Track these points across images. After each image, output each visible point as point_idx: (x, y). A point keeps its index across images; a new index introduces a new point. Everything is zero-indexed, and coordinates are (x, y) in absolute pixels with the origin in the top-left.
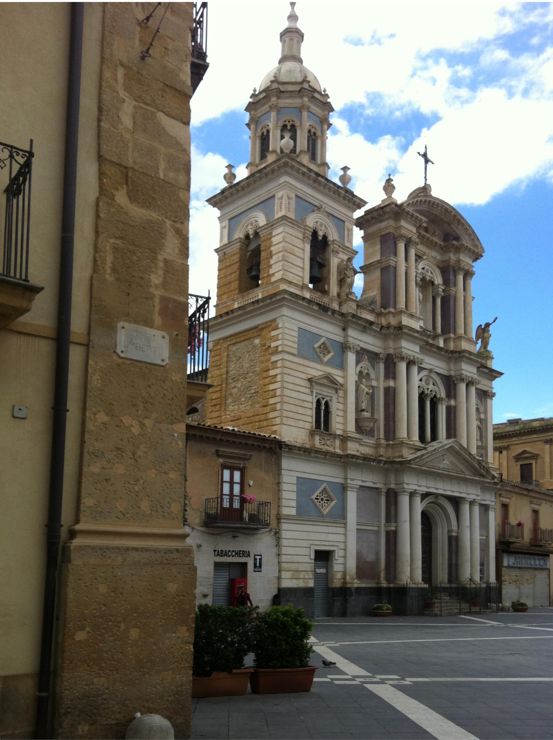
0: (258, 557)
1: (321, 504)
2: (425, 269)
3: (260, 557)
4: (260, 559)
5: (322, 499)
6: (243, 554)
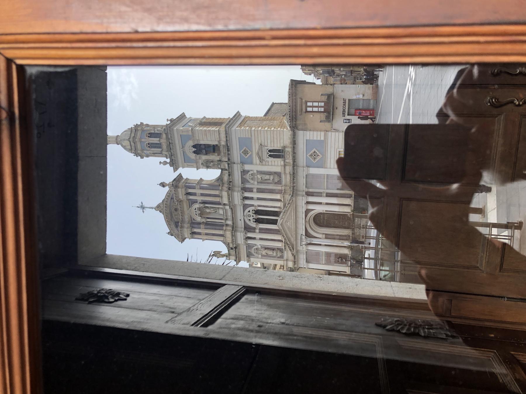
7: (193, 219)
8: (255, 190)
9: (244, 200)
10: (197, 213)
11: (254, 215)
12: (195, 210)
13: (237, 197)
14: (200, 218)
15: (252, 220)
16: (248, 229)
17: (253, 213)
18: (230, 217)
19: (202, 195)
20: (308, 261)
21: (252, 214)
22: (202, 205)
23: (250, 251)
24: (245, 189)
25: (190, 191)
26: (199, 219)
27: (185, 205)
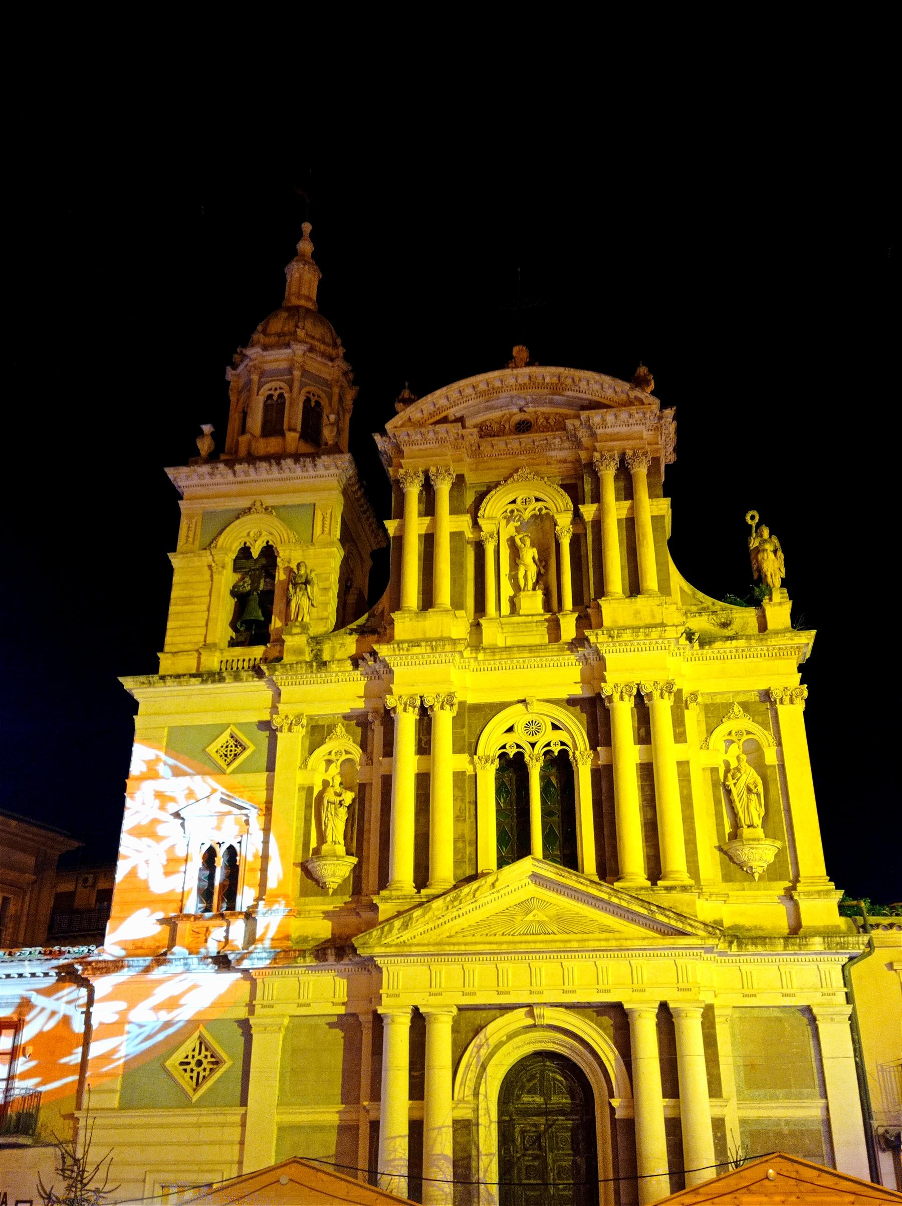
1: (195, 1075)
2: (519, 501)
15: (510, 739)
17: (548, 744)
23: (338, 729)
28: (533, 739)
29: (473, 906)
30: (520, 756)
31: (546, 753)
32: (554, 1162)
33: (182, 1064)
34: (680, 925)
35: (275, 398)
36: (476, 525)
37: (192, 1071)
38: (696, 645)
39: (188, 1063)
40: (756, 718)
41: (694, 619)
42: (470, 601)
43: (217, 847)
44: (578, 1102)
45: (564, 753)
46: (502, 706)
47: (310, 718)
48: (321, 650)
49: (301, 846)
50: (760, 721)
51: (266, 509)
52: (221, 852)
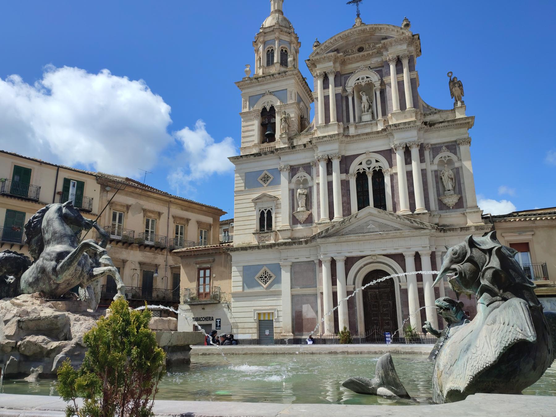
0: (218, 321)
1: (265, 280)
2: (360, 79)
3: (220, 320)
4: (220, 322)
5: (266, 277)
6: (209, 319)
7: (349, 76)
8: (424, 166)
9: (404, 149)
10: (360, 80)
11: (371, 170)
12: (365, 78)
13: (411, 136)
14: (353, 86)
15: (361, 167)
16: (346, 162)
17: (375, 168)
18: (360, 131)
19: (400, 84)
20: (293, 265)
21: (372, 166)
22: (377, 85)
23: (301, 169)
24: (422, 148)
25: (405, 63)
26: (351, 83)
27: (375, 61)
28: (369, 166)
29: (350, 224)
30: (364, 172)
31: (374, 171)
32: (382, 303)
33: (260, 277)
34: (422, 226)
35: (270, 51)
36: (345, 90)
37: (264, 279)
38: (428, 126)
39: (263, 277)
40: (452, 151)
41: (428, 116)
42: (345, 119)
43: (264, 211)
44: (389, 284)
45: (380, 171)
46: (358, 155)
47: (291, 166)
48: (293, 142)
49: (291, 209)
50: (453, 152)
51: (270, 93)
52: (266, 212)
